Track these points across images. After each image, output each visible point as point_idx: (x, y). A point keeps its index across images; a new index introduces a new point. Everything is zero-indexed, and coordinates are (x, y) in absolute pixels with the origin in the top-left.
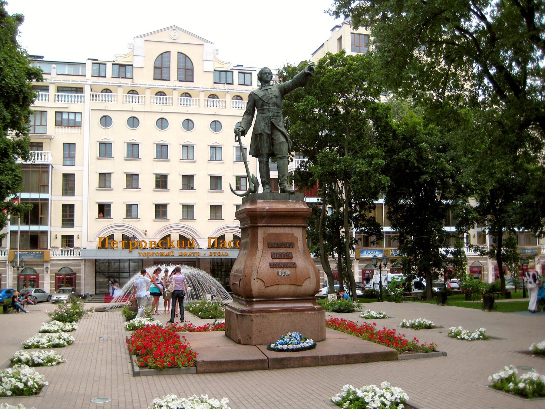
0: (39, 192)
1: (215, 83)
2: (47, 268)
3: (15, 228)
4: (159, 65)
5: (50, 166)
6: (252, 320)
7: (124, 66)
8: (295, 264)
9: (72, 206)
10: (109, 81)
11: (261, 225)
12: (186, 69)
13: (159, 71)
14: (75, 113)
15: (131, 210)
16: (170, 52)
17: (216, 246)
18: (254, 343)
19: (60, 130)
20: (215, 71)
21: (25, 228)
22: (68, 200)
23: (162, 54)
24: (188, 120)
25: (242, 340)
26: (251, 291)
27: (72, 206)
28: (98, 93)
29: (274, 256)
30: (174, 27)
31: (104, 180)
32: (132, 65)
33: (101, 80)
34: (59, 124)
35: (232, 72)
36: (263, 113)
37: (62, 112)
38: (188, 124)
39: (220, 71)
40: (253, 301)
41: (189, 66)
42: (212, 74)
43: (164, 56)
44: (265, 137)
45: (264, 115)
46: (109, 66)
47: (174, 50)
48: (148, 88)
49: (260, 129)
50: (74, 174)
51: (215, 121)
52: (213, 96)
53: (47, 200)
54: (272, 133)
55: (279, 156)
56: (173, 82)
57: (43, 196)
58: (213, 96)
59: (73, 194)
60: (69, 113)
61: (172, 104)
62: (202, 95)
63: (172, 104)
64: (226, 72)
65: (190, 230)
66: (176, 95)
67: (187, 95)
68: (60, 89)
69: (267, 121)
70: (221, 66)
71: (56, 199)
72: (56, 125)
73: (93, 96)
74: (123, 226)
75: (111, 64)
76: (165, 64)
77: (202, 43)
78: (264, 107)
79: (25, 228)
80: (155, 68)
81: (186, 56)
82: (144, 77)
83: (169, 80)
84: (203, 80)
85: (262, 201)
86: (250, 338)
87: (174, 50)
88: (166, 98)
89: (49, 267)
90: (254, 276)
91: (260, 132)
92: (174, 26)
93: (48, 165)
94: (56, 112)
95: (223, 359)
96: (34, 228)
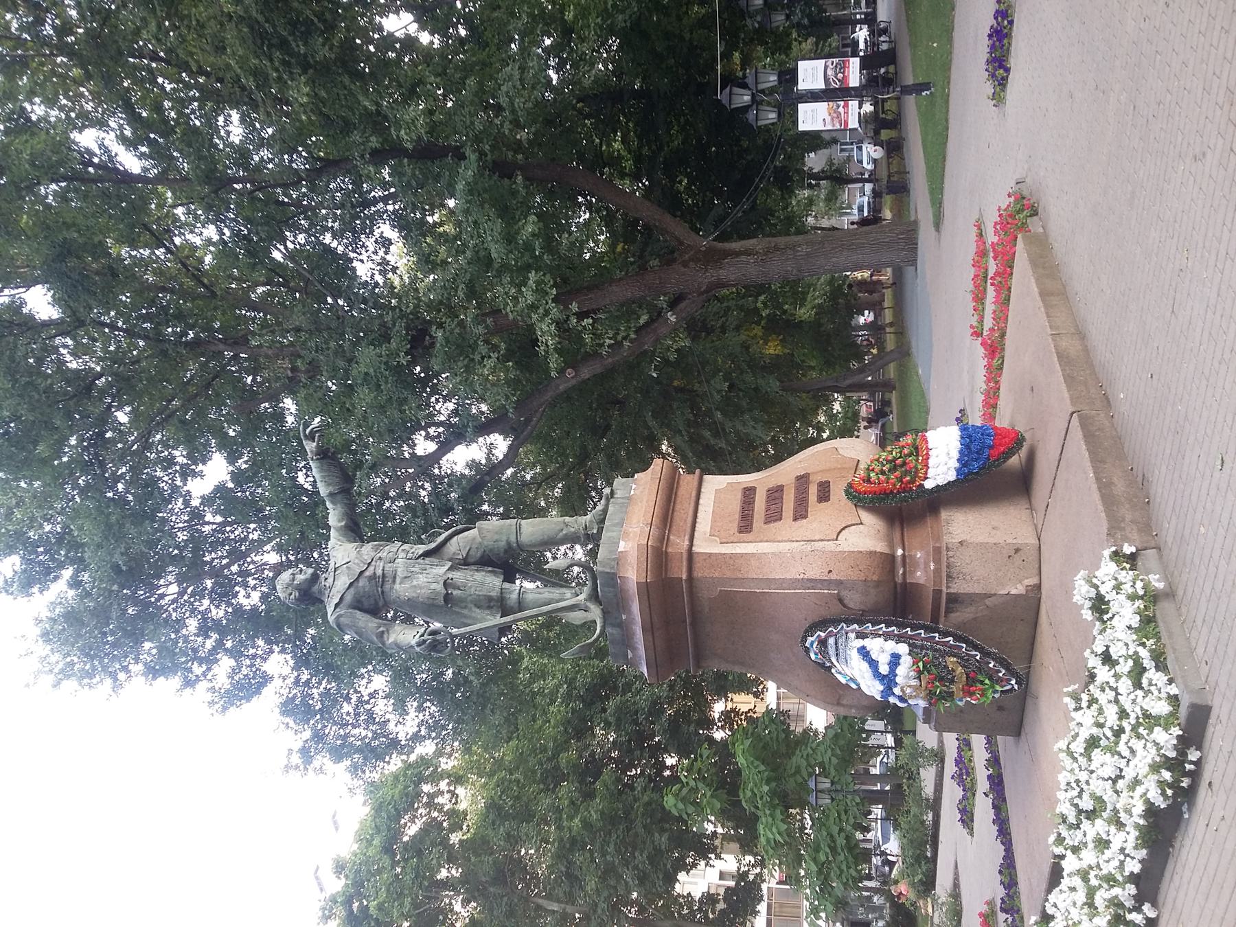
6: (961, 543)
8: (799, 478)
11: (687, 543)
18: (1035, 541)
25: (1028, 582)
26: (872, 554)
29: (774, 515)
36: (395, 577)
40: (904, 555)
44: (458, 576)
45: (400, 574)
49: (433, 586)
54: (450, 560)
55: (513, 539)
69: (416, 569)
78: (379, 572)
85: (622, 544)
86: (1017, 551)
90: (831, 546)
91: (439, 587)
95: (1096, 496)
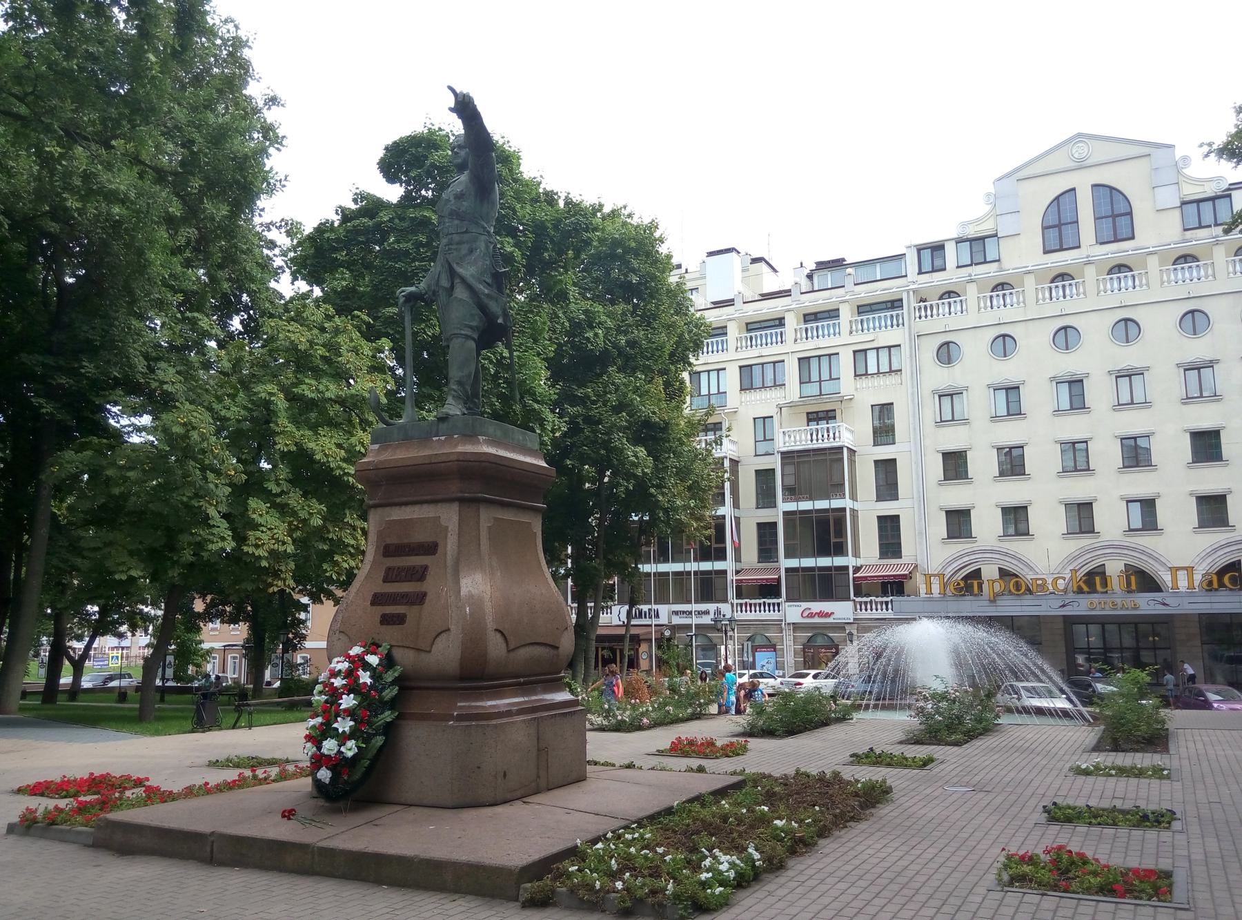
0: (828, 497)
1: (1185, 230)
2: (851, 634)
3: (793, 563)
4: (1052, 220)
5: (845, 450)
7: (982, 239)
9: (896, 519)
10: (951, 276)
12: (1114, 216)
13: (1053, 233)
14: (889, 347)
15: (1016, 518)
16: (1074, 189)
17: (1215, 585)
19: (864, 383)
20: (1184, 203)
21: (808, 562)
22: (888, 508)
23: (1057, 198)
24: (1126, 320)
27: (896, 519)
28: (934, 303)
30: (1080, 137)
31: (955, 465)
32: (996, 235)
33: (938, 277)
34: (861, 374)
35: (1230, 196)
37: (865, 351)
38: (1127, 328)
39: (1198, 201)
41: (1121, 207)
42: (1177, 213)
43: (1063, 203)
46: (950, 249)
47: (1083, 183)
48: (1029, 272)
50: (894, 460)
51: (1192, 312)
52: (1186, 258)
53: (844, 510)
56: (1091, 246)
57: (836, 503)
58: (1186, 258)
59: (895, 497)
60: (877, 349)
61: (1084, 293)
62: (1153, 262)
63: (1084, 293)
64: (1213, 199)
65: (1143, 552)
66: (1090, 272)
67: (1120, 267)
68: (862, 309)
70: (1200, 189)
71: (863, 506)
72: (856, 375)
73: (920, 309)
74: (998, 552)
75: (953, 243)
76: (1067, 217)
77: (1145, 150)
79: (808, 562)
80: (1044, 228)
81: (1112, 188)
82: (1023, 252)
83: (1079, 247)
84: (1157, 229)
87: (1083, 183)
88: (1133, 277)
89: (855, 632)
92: (1079, 135)
93: (841, 448)
94: (855, 352)
96: (824, 562)
